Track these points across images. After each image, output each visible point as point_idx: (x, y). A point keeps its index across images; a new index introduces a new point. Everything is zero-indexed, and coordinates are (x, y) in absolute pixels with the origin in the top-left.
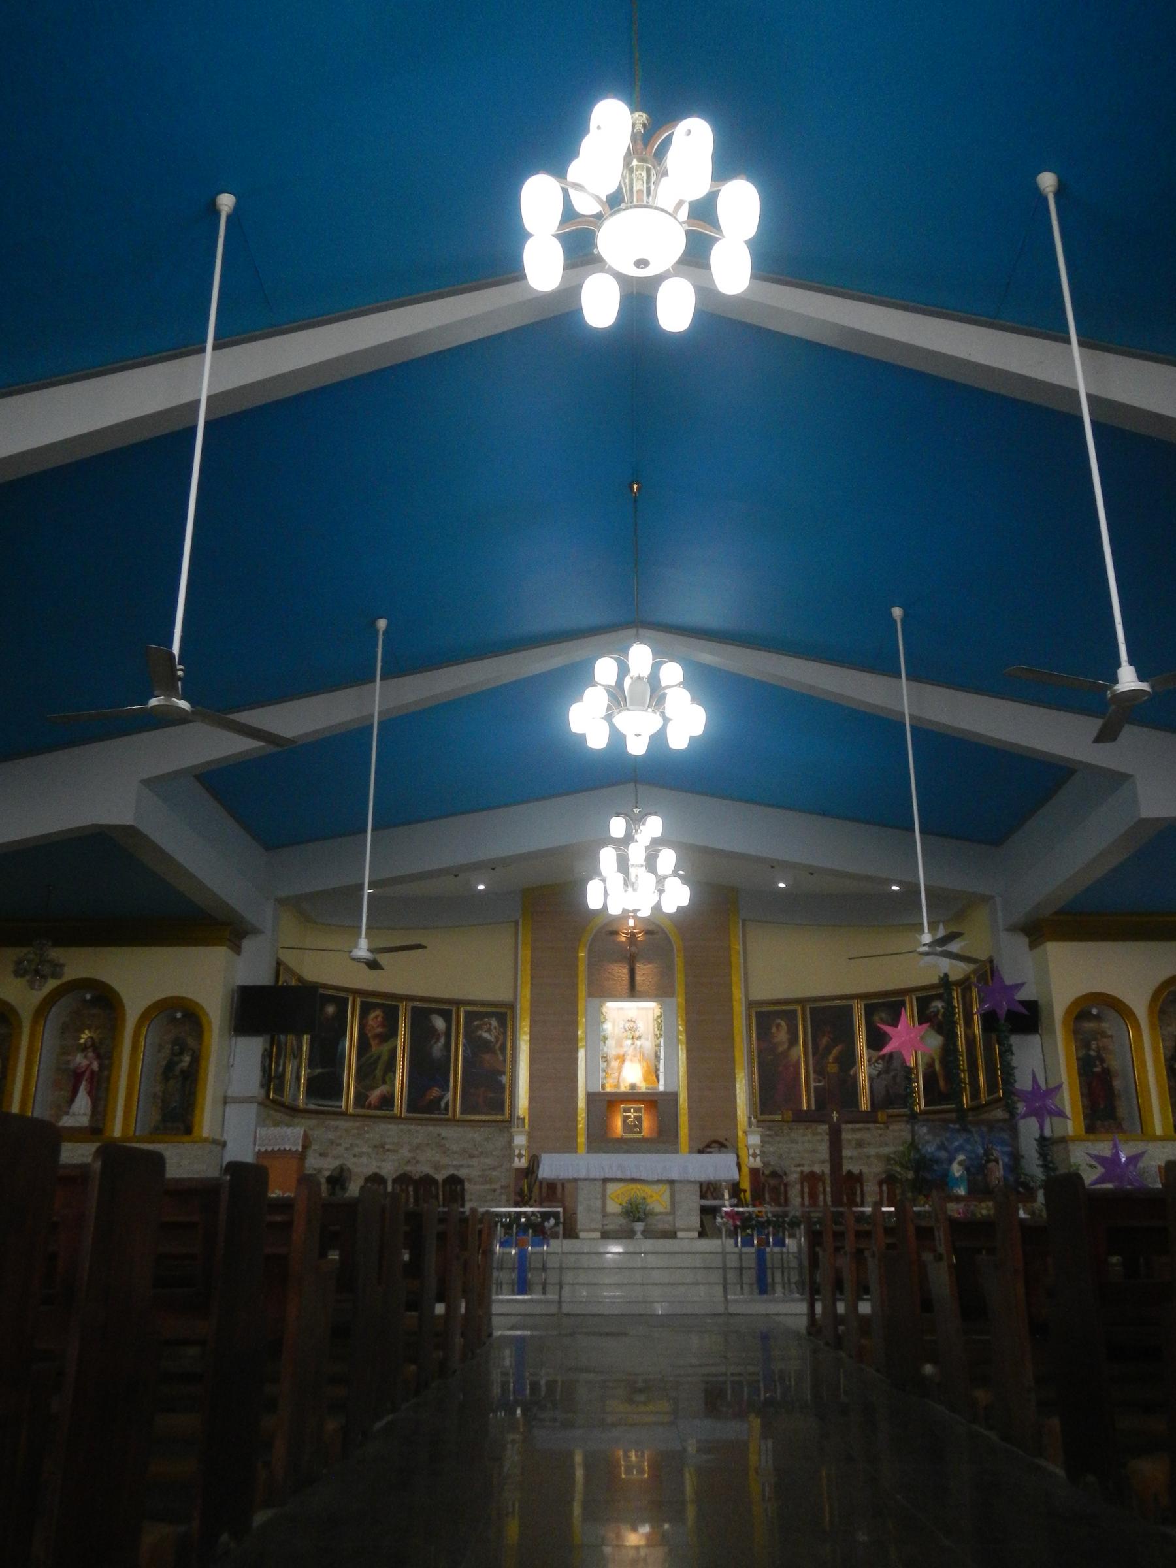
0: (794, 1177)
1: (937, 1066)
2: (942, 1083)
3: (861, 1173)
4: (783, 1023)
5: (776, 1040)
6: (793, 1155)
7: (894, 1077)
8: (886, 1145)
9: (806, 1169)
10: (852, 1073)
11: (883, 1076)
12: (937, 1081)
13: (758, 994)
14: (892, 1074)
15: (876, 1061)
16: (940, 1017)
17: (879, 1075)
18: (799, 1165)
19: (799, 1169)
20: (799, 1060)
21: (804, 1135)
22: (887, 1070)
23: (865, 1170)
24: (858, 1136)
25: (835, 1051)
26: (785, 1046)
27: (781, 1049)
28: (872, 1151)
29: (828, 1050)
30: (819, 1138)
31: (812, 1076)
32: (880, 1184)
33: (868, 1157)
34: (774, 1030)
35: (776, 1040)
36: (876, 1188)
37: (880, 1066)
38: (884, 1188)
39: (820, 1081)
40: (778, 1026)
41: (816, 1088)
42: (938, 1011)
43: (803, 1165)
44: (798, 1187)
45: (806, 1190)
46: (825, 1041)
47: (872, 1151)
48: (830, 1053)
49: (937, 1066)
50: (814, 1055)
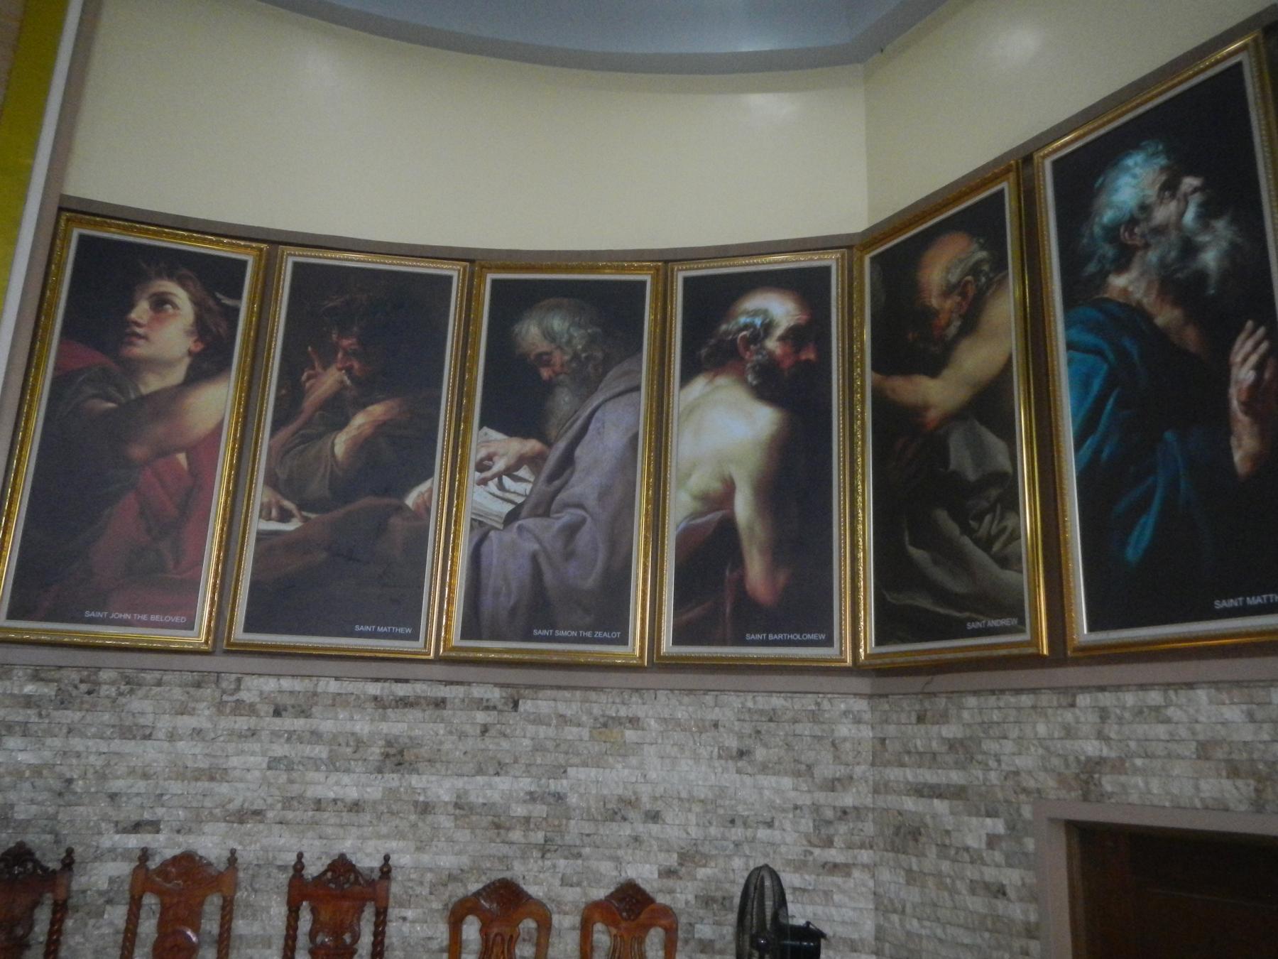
0: (103, 874)
1: (743, 508)
2: (756, 569)
3: (386, 871)
4: (181, 297)
5: (141, 350)
6: (117, 785)
7: (572, 530)
8: (501, 769)
9: (165, 846)
10: (411, 500)
11: (530, 523)
12: (738, 561)
13: (96, 181)
14: (567, 517)
15: (509, 471)
16: (772, 344)
17: (511, 517)
18: (137, 827)
19: (133, 842)
20: (217, 432)
21: (183, 711)
22: (543, 507)
23: (403, 859)
24: (398, 725)
25: (360, 421)
26: (177, 375)
27: (152, 383)
28: (440, 788)
29: (336, 412)
30: (242, 723)
31: (261, 493)
32: (456, 920)
33: (425, 809)
34: (141, 312)
35: (141, 350)
36: (441, 933)
37: (520, 488)
38: (471, 930)
39: (285, 516)
40: (160, 302)
41: (262, 536)
42: (768, 327)
43: (155, 826)
44: (117, 915)
45: (148, 927)
46: (329, 380)
47: (440, 788)
48: (342, 424)
49: (743, 508)
50: (277, 425)
